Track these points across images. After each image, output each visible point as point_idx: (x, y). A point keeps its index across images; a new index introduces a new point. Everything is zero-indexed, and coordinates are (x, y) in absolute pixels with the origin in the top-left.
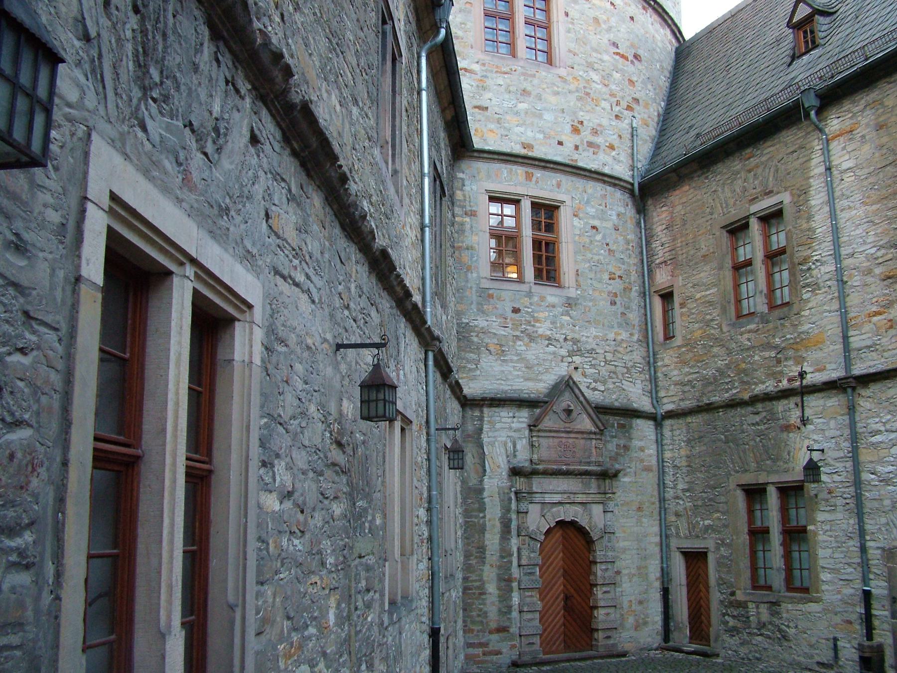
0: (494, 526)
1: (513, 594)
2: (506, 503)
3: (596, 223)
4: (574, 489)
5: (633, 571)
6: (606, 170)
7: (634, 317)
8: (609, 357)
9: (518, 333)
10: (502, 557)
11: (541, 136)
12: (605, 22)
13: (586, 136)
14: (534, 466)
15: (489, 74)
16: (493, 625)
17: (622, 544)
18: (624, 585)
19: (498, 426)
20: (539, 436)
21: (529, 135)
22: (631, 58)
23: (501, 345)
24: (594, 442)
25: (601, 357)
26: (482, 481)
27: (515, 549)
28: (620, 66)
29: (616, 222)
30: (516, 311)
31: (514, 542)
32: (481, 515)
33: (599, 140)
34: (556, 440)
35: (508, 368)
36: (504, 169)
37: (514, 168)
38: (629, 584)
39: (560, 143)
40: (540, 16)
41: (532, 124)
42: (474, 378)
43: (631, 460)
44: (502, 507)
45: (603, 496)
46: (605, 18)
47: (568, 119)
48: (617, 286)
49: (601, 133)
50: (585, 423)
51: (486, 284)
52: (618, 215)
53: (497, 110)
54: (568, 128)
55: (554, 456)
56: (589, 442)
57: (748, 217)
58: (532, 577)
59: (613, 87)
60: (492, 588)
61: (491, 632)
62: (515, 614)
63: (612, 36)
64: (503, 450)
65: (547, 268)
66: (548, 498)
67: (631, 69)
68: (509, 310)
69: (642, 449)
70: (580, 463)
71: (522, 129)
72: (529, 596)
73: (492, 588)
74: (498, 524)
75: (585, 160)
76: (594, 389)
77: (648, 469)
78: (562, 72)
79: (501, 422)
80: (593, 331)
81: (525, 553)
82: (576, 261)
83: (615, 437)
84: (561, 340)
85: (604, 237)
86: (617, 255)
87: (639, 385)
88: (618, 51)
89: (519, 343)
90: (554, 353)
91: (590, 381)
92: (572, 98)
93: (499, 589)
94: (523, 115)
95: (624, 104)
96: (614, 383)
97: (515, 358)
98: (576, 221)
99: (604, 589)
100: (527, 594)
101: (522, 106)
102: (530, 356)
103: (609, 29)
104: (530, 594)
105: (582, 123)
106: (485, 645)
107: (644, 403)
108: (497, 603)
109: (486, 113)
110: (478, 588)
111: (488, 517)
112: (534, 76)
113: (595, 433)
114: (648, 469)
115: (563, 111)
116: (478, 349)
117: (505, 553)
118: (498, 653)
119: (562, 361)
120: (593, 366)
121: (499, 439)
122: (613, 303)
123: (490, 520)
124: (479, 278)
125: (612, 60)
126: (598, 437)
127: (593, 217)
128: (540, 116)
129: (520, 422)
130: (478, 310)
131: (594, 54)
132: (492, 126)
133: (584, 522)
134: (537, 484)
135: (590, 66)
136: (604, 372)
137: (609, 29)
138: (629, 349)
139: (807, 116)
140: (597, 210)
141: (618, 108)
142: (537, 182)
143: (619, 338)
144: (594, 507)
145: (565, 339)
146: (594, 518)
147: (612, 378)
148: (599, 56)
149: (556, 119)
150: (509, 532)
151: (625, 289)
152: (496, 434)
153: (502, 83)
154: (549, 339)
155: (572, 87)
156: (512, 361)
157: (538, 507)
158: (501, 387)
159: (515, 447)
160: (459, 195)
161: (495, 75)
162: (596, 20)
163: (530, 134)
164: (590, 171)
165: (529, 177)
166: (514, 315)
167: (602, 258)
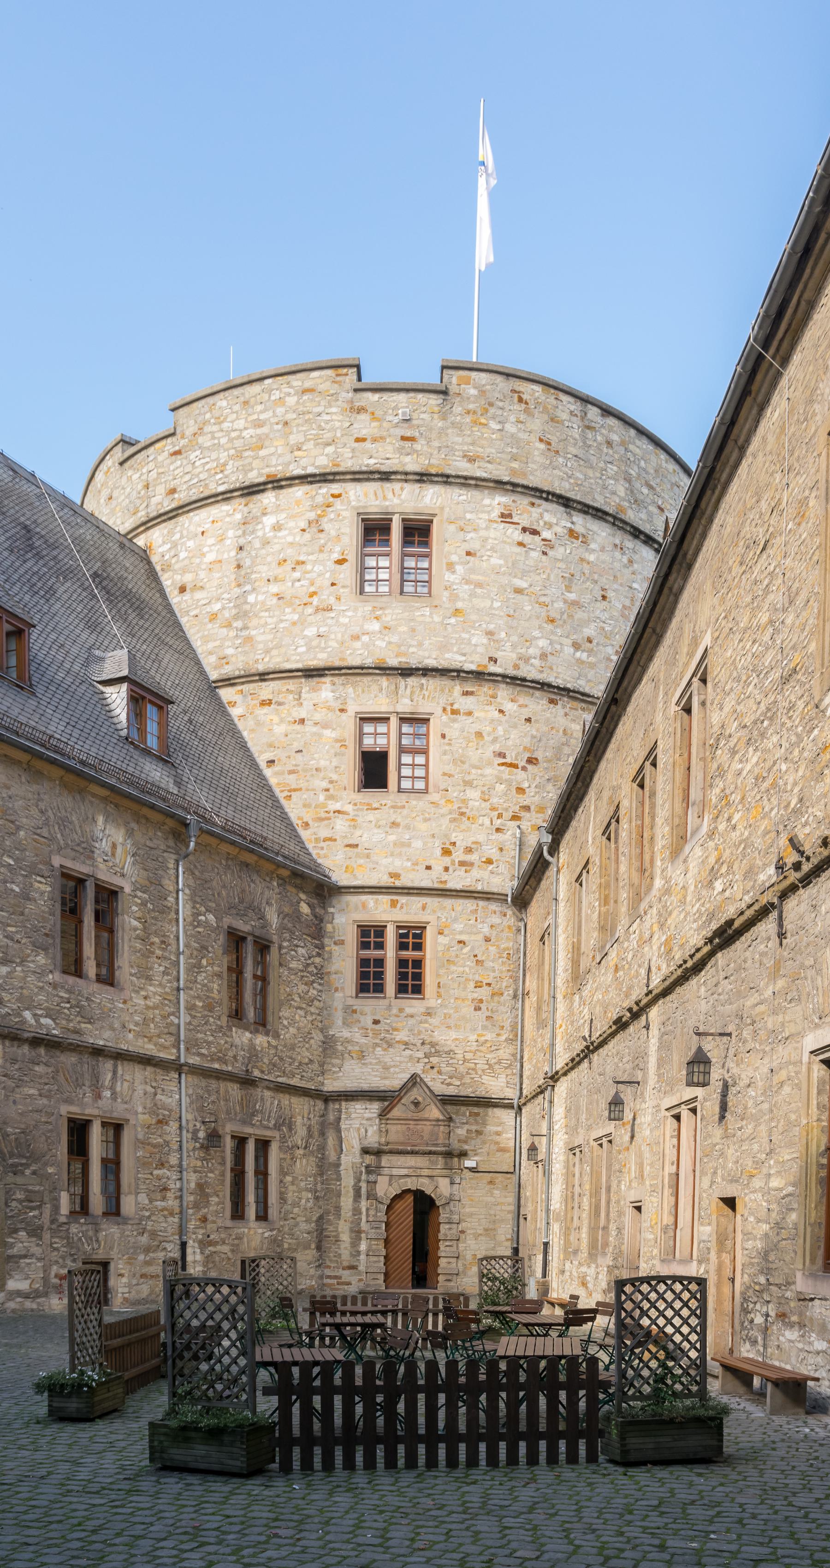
0: (348, 1192)
3: (463, 937)
4: (419, 1165)
5: (479, 1232)
8: (469, 1056)
9: (378, 1041)
10: (354, 1215)
11: (409, 864)
12: (489, 734)
15: (360, 813)
16: (345, 1264)
17: (467, 1210)
19: (353, 1116)
21: (398, 864)
24: (442, 1128)
26: (339, 1158)
27: (364, 1210)
28: (505, 776)
29: (488, 934)
30: (376, 1022)
31: (364, 1204)
33: (473, 857)
35: (367, 1070)
37: (380, 897)
39: (428, 868)
41: (400, 854)
42: (338, 1078)
43: (484, 1142)
50: (434, 1112)
51: (351, 1002)
53: (366, 845)
54: (438, 852)
55: (402, 1139)
59: (495, 800)
60: (345, 1237)
61: (344, 1269)
62: (363, 1257)
63: (497, 747)
64: (356, 1135)
66: (395, 1172)
67: (520, 775)
68: (369, 1022)
69: (498, 1134)
70: (427, 1145)
71: (390, 860)
73: (345, 1237)
75: (456, 881)
76: (449, 1084)
80: (453, 1035)
81: (372, 1212)
84: (419, 1044)
85: (473, 949)
87: (502, 1079)
88: (504, 761)
89: (379, 1049)
92: (445, 822)
95: (508, 815)
98: (442, 939)
99: (447, 1243)
101: (392, 838)
103: (495, 740)
105: (454, 844)
106: (340, 1278)
109: (356, 850)
110: (335, 1236)
112: (403, 807)
115: (433, 836)
117: (357, 1211)
118: (349, 1284)
120: (448, 1065)
122: (478, 1009)
124: (345, 997)
127: (461, 933)
128: (409, 845)
130: (344, 1023)
131: (474, 771)
132: (362, 861)
134: (385, 1160)
135: (468, 784)
137: (495, 740)
138: (493, 1048)
141: (499, 821)
142: (402, 907)
143: (483, 1039)
144: (440, 1180)
145: (423, 1044)
146: (440, 1188)
148: (479, 771)
149: (425, 844)
150: (360, 1196)
151: (493, 995)
154: (406, 1044)
155: (444, 810)
156: (371, 1064)
159: (366, 1131)
160: (329, 927)
162: (479, 735)
163: (398, 863)
165: (394, 904)
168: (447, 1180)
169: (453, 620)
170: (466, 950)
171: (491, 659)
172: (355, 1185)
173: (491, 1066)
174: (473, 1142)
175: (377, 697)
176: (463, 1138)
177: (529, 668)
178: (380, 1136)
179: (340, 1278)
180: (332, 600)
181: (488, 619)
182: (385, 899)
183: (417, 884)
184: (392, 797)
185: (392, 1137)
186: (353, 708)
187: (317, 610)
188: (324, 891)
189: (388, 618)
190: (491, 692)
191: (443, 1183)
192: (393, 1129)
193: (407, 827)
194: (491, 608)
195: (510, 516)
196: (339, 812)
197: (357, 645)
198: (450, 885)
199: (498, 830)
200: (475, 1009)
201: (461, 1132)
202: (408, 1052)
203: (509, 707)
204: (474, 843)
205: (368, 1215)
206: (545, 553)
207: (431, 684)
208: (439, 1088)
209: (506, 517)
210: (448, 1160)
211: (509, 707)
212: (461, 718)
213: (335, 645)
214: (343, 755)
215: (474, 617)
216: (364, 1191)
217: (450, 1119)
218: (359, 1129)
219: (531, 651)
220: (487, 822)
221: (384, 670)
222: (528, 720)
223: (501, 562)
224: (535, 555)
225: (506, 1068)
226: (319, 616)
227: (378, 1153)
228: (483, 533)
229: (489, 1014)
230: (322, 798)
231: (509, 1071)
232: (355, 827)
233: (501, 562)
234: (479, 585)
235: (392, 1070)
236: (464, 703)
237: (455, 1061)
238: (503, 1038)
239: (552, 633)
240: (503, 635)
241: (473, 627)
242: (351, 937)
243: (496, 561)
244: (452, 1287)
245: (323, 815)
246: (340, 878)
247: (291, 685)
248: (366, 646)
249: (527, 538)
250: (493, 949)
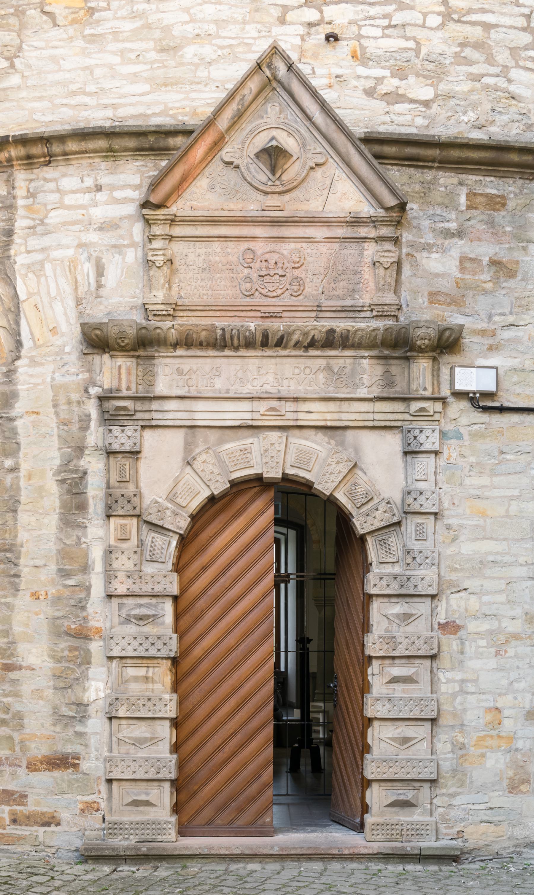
0: (40, 490)
1: (92, 672)
2: (75, 427)
4: (291, 388)
10: (64, 574)
14: (154, 323)
16: (40, 749)
17: (467, 548)
18: (473, 664)
20: (171, 238)
24: (370, 250)
27: (97, 554)
31: (97, 534)
32: (8, 463)
34: (236, 250)
38: (493, 663)
45: (399, 407)
50: (342, 194)
55: (226, 292)
56: (351, 250)
58: (149, 629)
60: (36, 655)
61: (32, 767)
62: (96, 725)
64: (67, 288)
66: (204, 413)
72: (136, 679)
74: (53, 488)
76: (394, 97)
79: (62, 206)
81: (124, 563)
83: (460, 234)
91: (378, 72)
96: (477, 78)
97: (128, 26)
99: (397, 671)
100: (131, 672)
104: (142, 672)
106: (21, 798)
108: (49, 693)
111: (24, 467)
113: (373, 221)
117: (72, 563)
118: (50, 821)
119: (282, 21)
121: (56, 254)
123: (29, 477)
126: (385, 231)
129: (117, 201)
134: (170, 373)
136: (437, 43)
144: (368, 440)
146: (367, 474)
147: (470, 63)
150: (82, 507)
152: (47, 241)
157: (175, 440)
158: (84, 114)
159: (100, 272)
168: (393, 443)
172: (66, 465)
174: (483, 304)
176: (445, 285)
178: (149, 284)
179: (21, 798)
191: (380, 453)
201: (441, 264)
205: (109, 574)
210: (396, 368)
216: (94, 490)
218: (73, 264)
227: (143, 345)
235: (189, 52)
237: (415, 16)
244: (418, 831)
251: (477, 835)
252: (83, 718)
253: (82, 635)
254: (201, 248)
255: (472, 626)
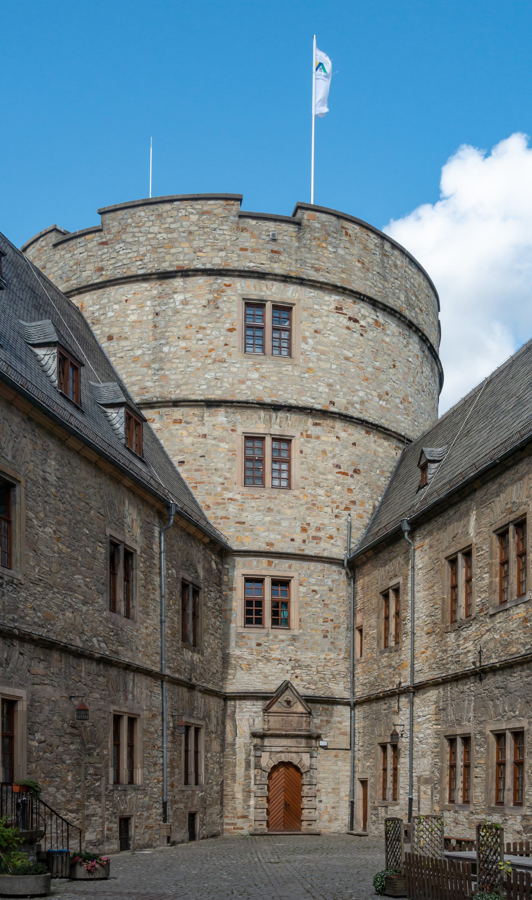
0: (241, 763)
3: (315, 588)
6: (325, 554)
7: (343, 643)
8: (320, 669)
9: (260, 658)
11: (280, 537)
12: (330, 452)
13: (312, 532)
15: (246, 501)
16: (239, 814)
17: (321, 775)
19: (245, 710)
21: (272, 537)
22: (350, 473)
23: (249, 665)
24: (304, 718)
25: (314, 669)
26: (234, 740)
27: (253, 776)
28: (341, 481)
30: (259, 645)
31: (253, 772)
33: (321, 534)
35: (253, 678)
36: (254, 561)
39: (292, 540)
40: (284, 455)
41: (274, 530)
43: (331, 729)
44: (246, 753)
46: (330, 449)
47: (298, 523)
48: (329, 626)
49: (323, 529)
50: (299, 708)
51: (241, 630)
52: (333, 581)
53: (251, 523)
54: (299, 529)
55: (278, 726)
56: (301, 718)
57: (388, 589)
59: (334, 496)
60: (239, 796)
61: (238, 818)
62: (252, 809)
63: (335, 461)
64: (247, 723)
65: (280, 619)
66: (274, 749)
67: (350, 480)
68: (254, 644)
69: (340, 723)
70: (295, 730)
71: (267, 534)
73: (239, 796)
74: (243, 763)
75: (311, 550)
76: (308, 688)
77: (344, 734)
78: (296, 492)
80: (310, 654)
81: (258, 778)
82: (299, 613)
83: (320, 715)
84: (287, 661)
85: (321, 596)
86: (331, 606)
87: (342, 685)
88: (340, 470)
89: (261, 663)
90: (282, 669)
92: (303, 509)
93: (243, 796)
94: (268, 524)
95: (342, 507)
97: (258, 672)
98: (302, 589)
99: (309, 799)
101: (268, 519)
102: (266, 671)
103: (334, 457)
105: (309, 524)
106: (236, 824)
107: (346, 695)
109: (243, 526)
110: (231, 795)
111: (238, 758)
112: (276, 498)
114: (344, 734)
115: (295, 518)
116: (235, 667)
117: (247, 777)
118: (242, 829)
120: (308, 675)
122: (325, 637)
124: (237, 627)
125: (335, 478)
127: (314, 585)
128: (279, 524)
130: (236, 645)
131: (321, 476)
132: (247, 534)
133: (296, 762)
134: (266, 742)
135: (317, 485)
136: (316, 678)
137: (334, 457)
138: (336, 664)
139: (403, 537)
140: (317, 580)
141: (337, 511)
142: (275, 566)
143: (328, 657)
144: (303, 754)
145: (290, 660)
148: (325, 477)
149: (290, 524)
150: (250, 767)
151: (335, 628)
153: (254, 505)
154: (279, 660)
155: (302, 502)
156: (255, 673)
159: (254, 721)
160: (225, 578)
161: (250, 501)
162: (324, 452)
163: (272, 536)
164: (311, 556)
165: (270, 564)
166: (257, 647)
167: (318, 610)
169: (306, 375)
170: (317, 597)
171: (331, 402)
172: (246, 759)
173: (334, 676)
175: (257, 423)
176: (318, 725)
177: (354, 410)
179: (236, 824)
180: (225, 355)
181: (328, 375)
182: (264, 561)
183: (284, 551)
184: (268, 491)
185: (272, 725)
186: (240, 429)
187: (214, 361)
188: (223, 552)
189: (264, 371)
190: (331, 424)
191: (306, 757)
192: (272, 719)
193: (279, 512)
194: (331, 368)
195: (341, 309)
196: (231, 499)
197: (243, 387)
198: (307, 552)
199: (336, 516)
200: (324, 637)
202: (280, 666)
203: (343, 435)
204: (321, 524)
205: (255, 780)
206: (362, 335)
207: (293, 418)
208: (302, 691)
209: (339, 309)
211: (343, 435)
212: (313, 440)
213: (228, 386)
214: (234, 460)
215: (320, 374)
217: (310, 713)
218: (248, 719)
219: (355, 399)
220: (329, 510)
221: (262, 405)
222: (354, 444)
223: (337, 339)
224: (356, 335)
225: (343, 677)
226: (216, 365)
227: (262, 736)
228: (325, 319)
229: (332, 640)
230: (219, 489)
231: (345, 680)
232: (242, 510)
233: (337, 339)
234: (323, 353)
235: (270, 678)
236: (314, 430)
237: (311, 672)
238: (341, 656)
239: (368, 388)
240: (338, 387)
241: (319, 381)
242: (239, 583)
243: (332, 338)
244: (312, 830)
245: (220, 501)
246: (235, 545)
247: (196, 411)
248: (249, 388)
249: (351, 324)
250: (334, 596)
251: (323, 831)
252: (249, 808)
253: (249, 792)
254: (273, 718)
255: (322, 790)
